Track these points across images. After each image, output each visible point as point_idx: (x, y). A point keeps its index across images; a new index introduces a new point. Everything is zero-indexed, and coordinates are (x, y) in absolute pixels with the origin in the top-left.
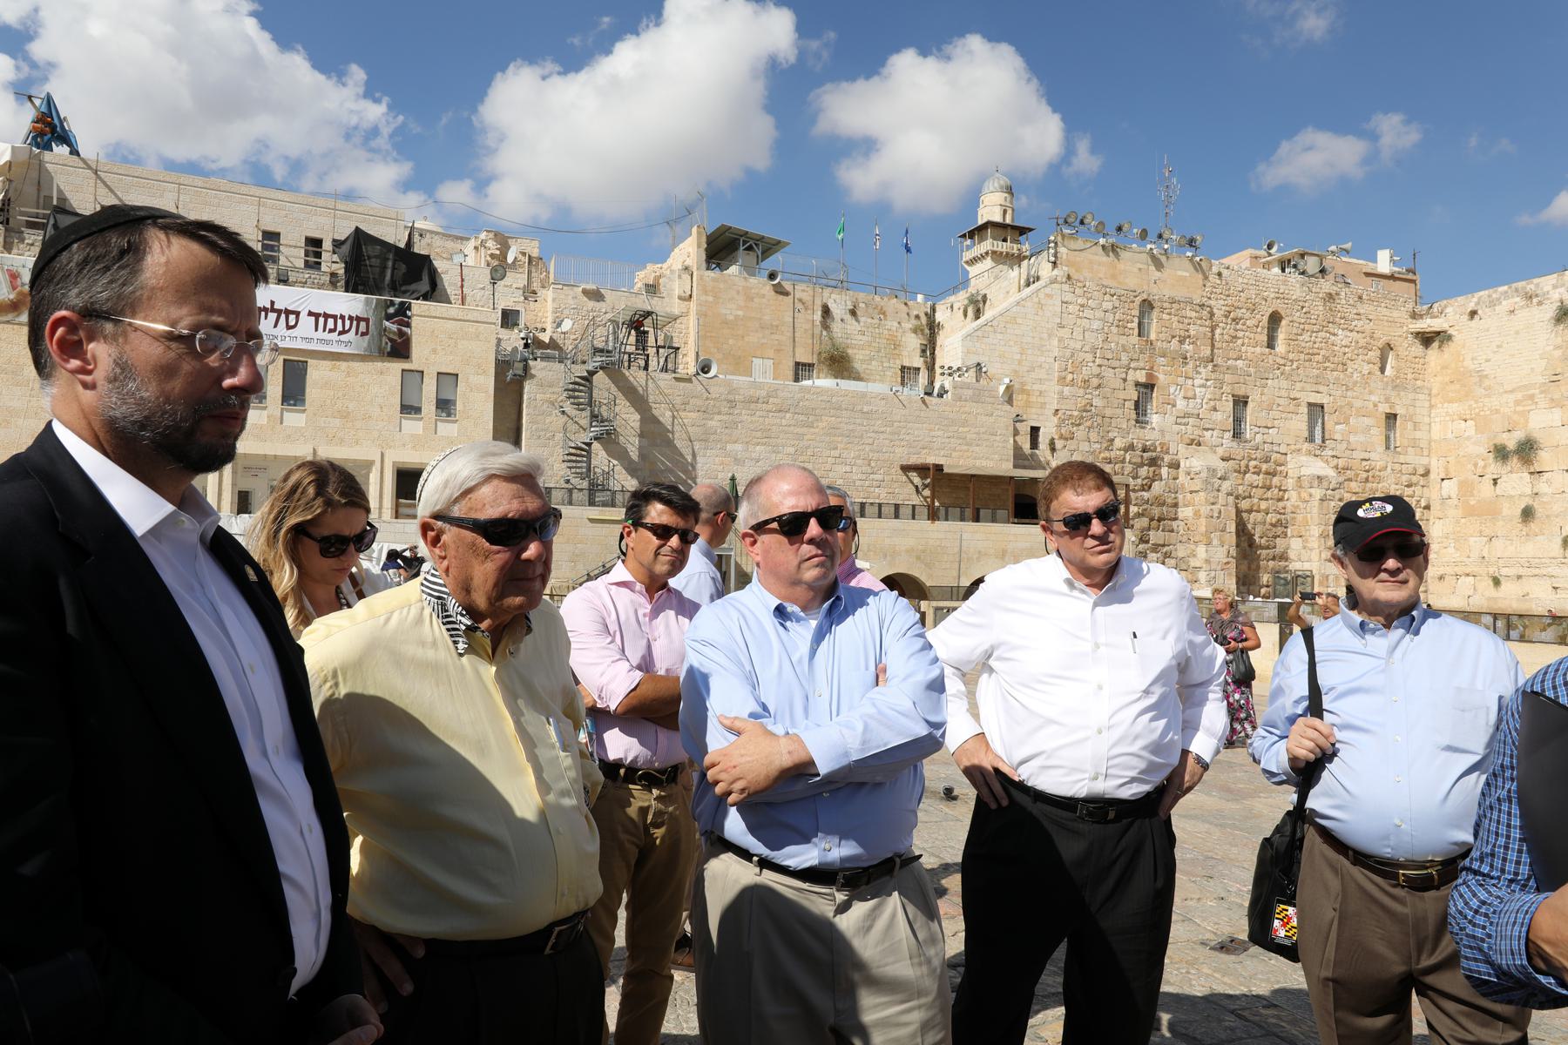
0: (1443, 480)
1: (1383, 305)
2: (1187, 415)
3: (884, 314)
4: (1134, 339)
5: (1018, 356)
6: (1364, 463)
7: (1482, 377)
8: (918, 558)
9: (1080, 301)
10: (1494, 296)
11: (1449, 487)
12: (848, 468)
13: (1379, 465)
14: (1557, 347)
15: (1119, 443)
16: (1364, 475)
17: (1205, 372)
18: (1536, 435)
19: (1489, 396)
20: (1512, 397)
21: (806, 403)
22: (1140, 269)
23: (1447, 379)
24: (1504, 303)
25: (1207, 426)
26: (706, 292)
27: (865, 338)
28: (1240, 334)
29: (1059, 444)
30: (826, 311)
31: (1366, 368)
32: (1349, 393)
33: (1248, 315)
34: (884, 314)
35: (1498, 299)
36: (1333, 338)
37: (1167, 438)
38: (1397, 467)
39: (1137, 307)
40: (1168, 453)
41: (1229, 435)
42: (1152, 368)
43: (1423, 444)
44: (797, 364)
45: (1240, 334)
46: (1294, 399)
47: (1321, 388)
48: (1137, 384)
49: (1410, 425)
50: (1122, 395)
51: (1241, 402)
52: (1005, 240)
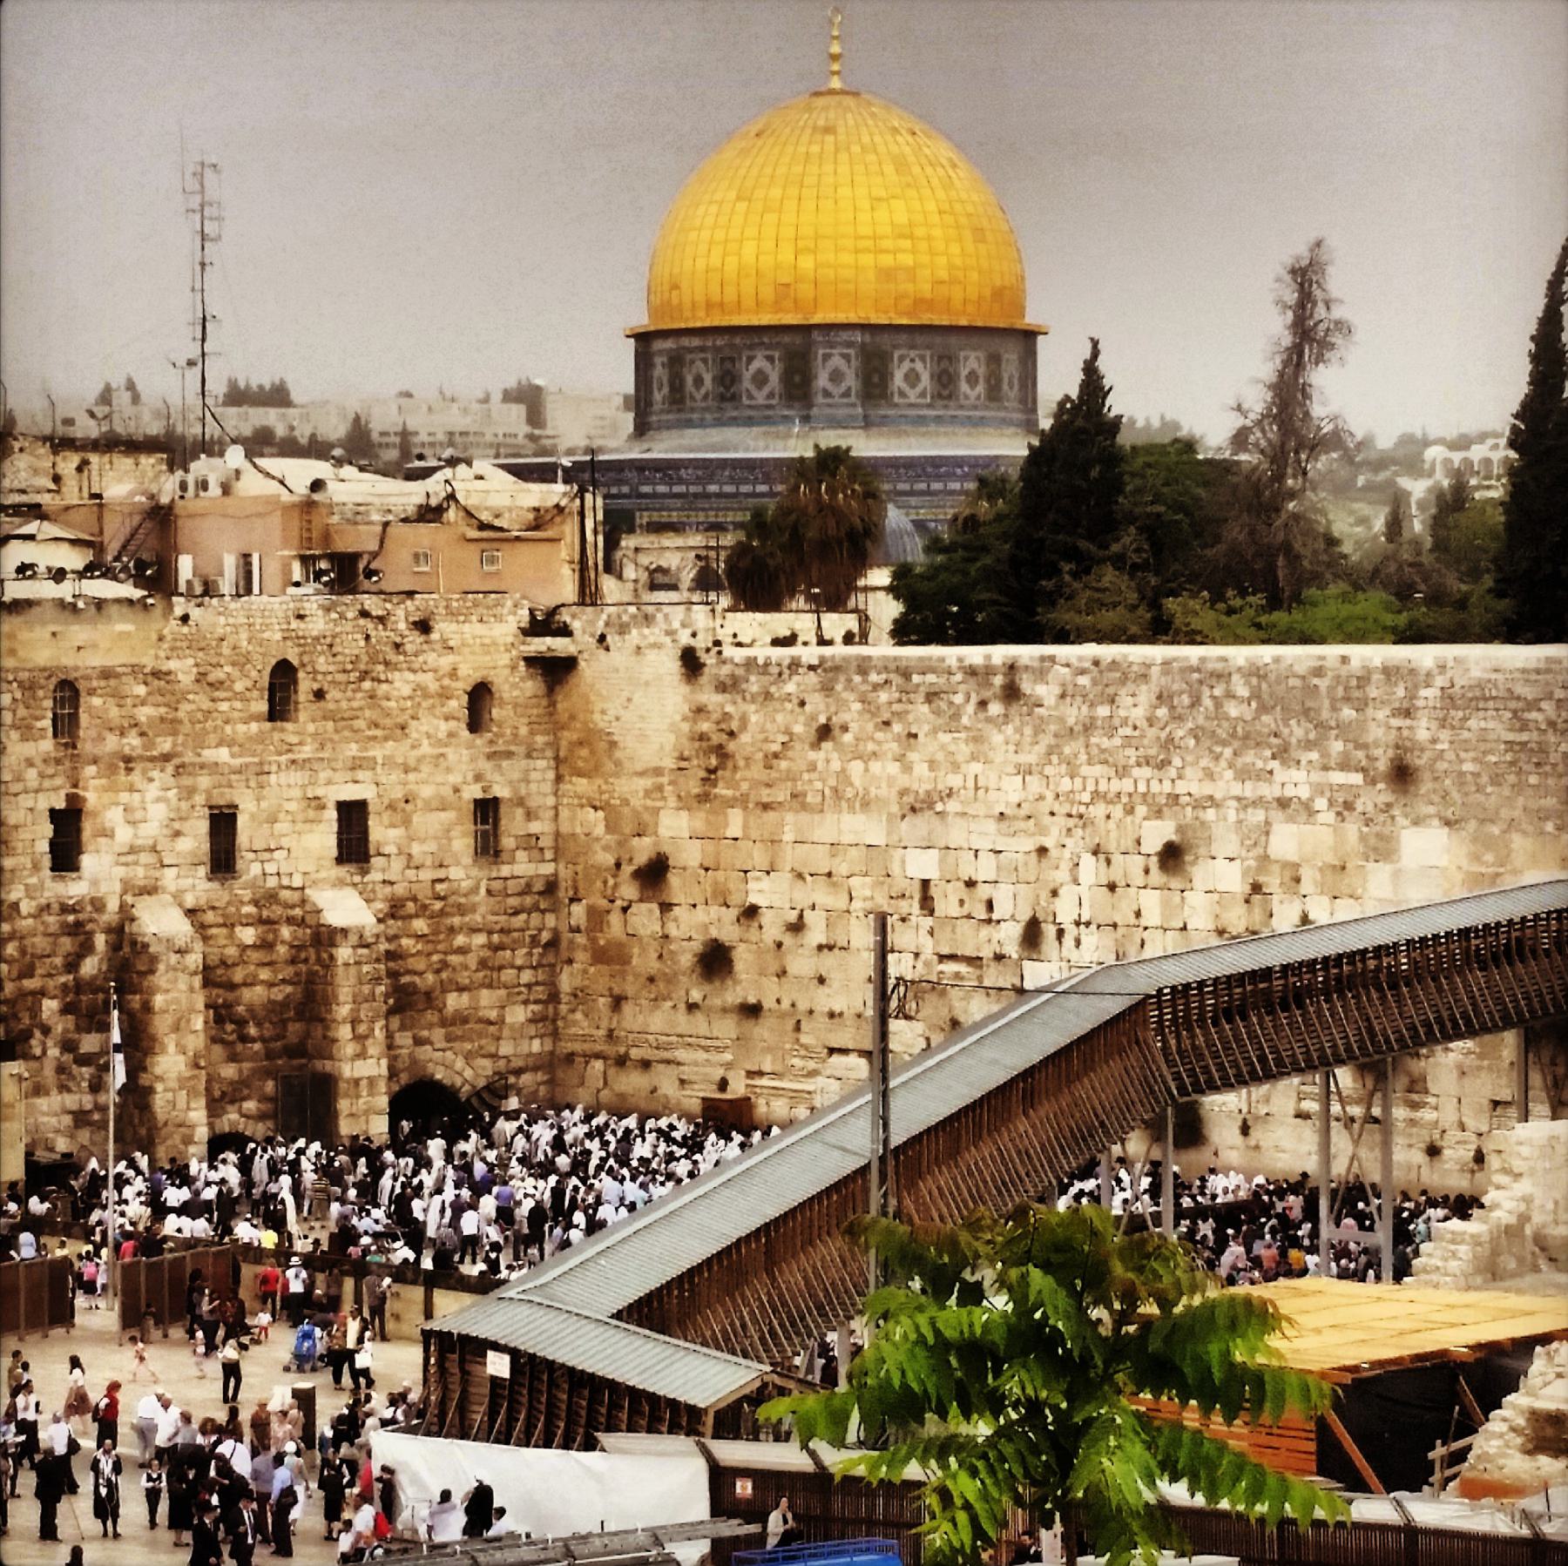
0: (572, 900)
1: (474, 618)
2: (133, 850)
4: (47, 745)
6: (439, 887)
10: (625, 618)
11: (578, 912)
13: (466, 885)
14: (685, 719)
15: (25, 907)
16: (438, 905)
17: (162, 776)
18: (666, 848)
19: (617, 775)
22: (54, 634)
23: (575, 737)
24: (634, 632)
25: (166, 862)
28: (224, 706)
31: (444, 727)
32: (412, 777)
33: (235, 672)
35: (628, 625)
36: (384, 686)
37: (103, 889)
38: (497, 885)
39: (50, 694)
41: (202, 871)
42: (75, 786)
46: (317, 798)
47: (360, 775)
49: (520, 812)
51: (223, 823)
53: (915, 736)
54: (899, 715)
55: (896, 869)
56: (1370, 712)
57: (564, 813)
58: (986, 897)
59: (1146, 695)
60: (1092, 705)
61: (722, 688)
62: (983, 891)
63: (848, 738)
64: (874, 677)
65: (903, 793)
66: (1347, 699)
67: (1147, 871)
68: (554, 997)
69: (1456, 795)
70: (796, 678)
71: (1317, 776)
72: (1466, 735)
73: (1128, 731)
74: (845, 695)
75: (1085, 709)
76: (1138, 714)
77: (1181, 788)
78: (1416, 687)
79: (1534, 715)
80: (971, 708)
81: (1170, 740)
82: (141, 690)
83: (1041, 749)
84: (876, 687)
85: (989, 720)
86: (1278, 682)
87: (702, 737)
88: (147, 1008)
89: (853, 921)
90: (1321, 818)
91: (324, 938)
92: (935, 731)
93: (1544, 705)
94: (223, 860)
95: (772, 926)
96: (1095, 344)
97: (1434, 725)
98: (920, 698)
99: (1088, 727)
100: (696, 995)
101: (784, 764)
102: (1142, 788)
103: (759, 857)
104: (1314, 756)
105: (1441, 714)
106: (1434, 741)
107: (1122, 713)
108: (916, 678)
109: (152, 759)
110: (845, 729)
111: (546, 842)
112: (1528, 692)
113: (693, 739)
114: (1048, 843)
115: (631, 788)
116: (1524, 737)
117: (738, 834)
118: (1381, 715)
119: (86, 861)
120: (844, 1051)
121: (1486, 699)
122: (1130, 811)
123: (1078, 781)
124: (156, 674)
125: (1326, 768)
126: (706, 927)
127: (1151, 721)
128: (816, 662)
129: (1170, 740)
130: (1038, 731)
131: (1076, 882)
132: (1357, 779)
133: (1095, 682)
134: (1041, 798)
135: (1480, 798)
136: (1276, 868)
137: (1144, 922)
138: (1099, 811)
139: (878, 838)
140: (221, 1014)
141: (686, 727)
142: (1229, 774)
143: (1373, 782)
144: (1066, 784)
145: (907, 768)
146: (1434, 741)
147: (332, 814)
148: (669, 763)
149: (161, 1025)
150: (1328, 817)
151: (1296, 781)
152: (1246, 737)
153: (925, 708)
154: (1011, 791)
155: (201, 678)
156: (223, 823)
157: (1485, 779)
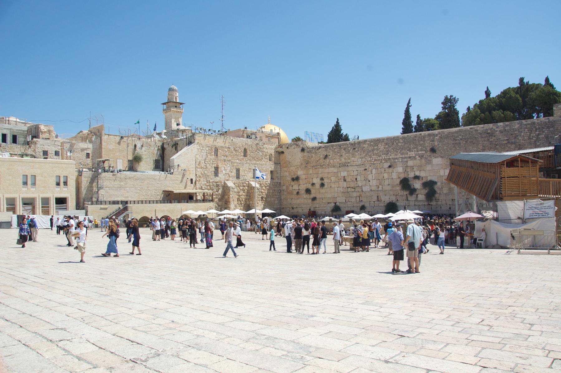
2: (226, 174)
3: (151, 146)
4: (213, 157)
5: (187, 162)
7: (290, 163)
8: (169, 212)
9: (201, 148)
11: (284, 188)
12: (152, 192)
14: (302, 157)
19: (291, 167)
20: (294, 168)
21: (142, 178)
23: (283, 162)
26: (105, 142)
27: (146, 152)
28: (238, 154)
29: (197, 182)
30: (135, 146)
34: (151, 146)
40: (221, 183)
41: (235, 178)
43: (279, 177)
44: (129, 160)
45: (238, 154)
48: (214, 167)
49: (276, 173)
50: (211, 170)
51: (238, 171)
52: (176, 107)
53: (342, 155)
54: (339, 153)
55: (339, 175)
56: (426, 142)
57: (282, 173)
58: (356, 177)
59: (383, 144)
60: (374, 147)
61: (308, 152)
62: (355, 177)
63: (330, 157)
64: (334, 147)
65: (340, 164)
66: (421, 140)
67: (385, 170)
68: (281, 199)
69: (443, 153)
70: (321, 149)
71: (416, 153)
72: (444, 143)
73: (380, 150)
74: (330, 151)
75: (372, 147)
76: (383, 147)
77: (391, 157)
78: (435, 137)
79: (458, 138)
80: (352, 150)
81: (388, 150)
82: (226, 150)
83: (365, 154)
84: (335, 149)
85: (355, 151)
86: (408, 139)
87: (305, 160)
88: (229, 198)
89: (332, 183)
90: (417, 159)
91: (251, 188)
92: (345, 154)
93: (460, 137)
94: (238, 177)
95: (318, 186)
96: (338, 119)
97: (438, 142)
98: (343, 149)
99: (373, 150)
100: (305, 197)
101: (319, 162)
102: (383, 158)
103: (315, 176)
104: (415, 150)
105: (439, 140)
106: (438, 144)
107: (379, 147)
108: (342, 147)
109: (228, 160)
110: (329, 155)
111: (279, 177)
112: (456, 135)
113: (303, 160)
114: (367, 168)
115: (293, 169)
116: (456, 142)
117: (311, 173)
118: (428, 142)
119: (219, 175)
120: (330, 203)
121: (448, 137)
122: (381, 162)
123: (372, 159)
124: (229, 148)
125: (418, 151)
126: (307, 187)
127: (385, 148)
128: (324, 146)
129: (388, 150)
130: (364, 152)
131: (372, 174)
132: (424, 152)
133: (374, 143)
134: (365, 162)
135: (448, 152)
136: (409, 167)
137: (384, 178)
138: (376, 162)
139: (335, 170)
140: (238, 200)
141: (302, 159)
142: (400, 154)
143: (427, 152)
144: (369, 159)
145: (341, 160)
146: (438, 144)
147: (252, 171)
148: (299, 164)
149: (231, 200)
150: (419, 159)
151: (412, 154)
152: (402, 148)
153: (344, 151)
154: (360, 162)
155: (234, 149)
156: (238, 171)
157: (448, 149)
